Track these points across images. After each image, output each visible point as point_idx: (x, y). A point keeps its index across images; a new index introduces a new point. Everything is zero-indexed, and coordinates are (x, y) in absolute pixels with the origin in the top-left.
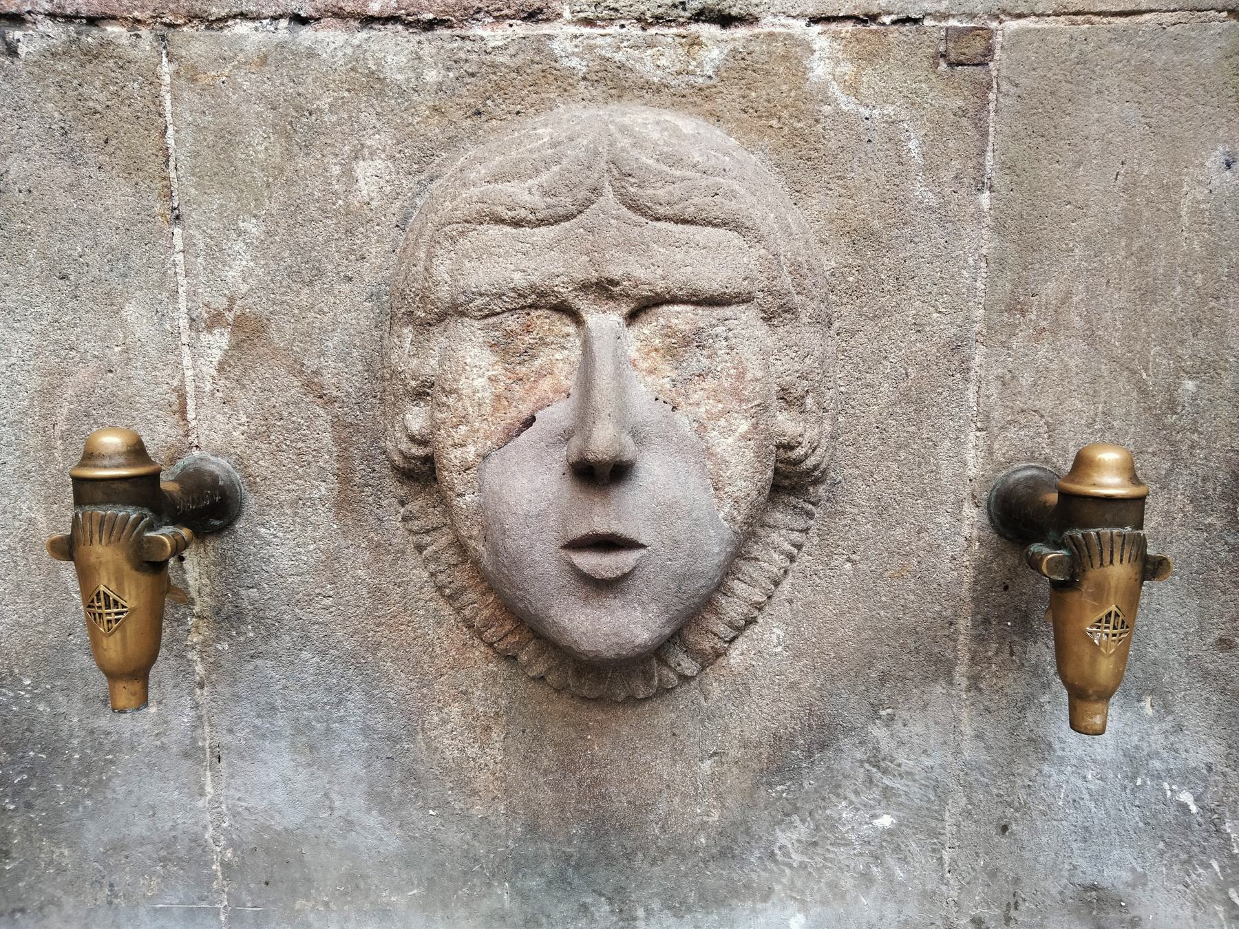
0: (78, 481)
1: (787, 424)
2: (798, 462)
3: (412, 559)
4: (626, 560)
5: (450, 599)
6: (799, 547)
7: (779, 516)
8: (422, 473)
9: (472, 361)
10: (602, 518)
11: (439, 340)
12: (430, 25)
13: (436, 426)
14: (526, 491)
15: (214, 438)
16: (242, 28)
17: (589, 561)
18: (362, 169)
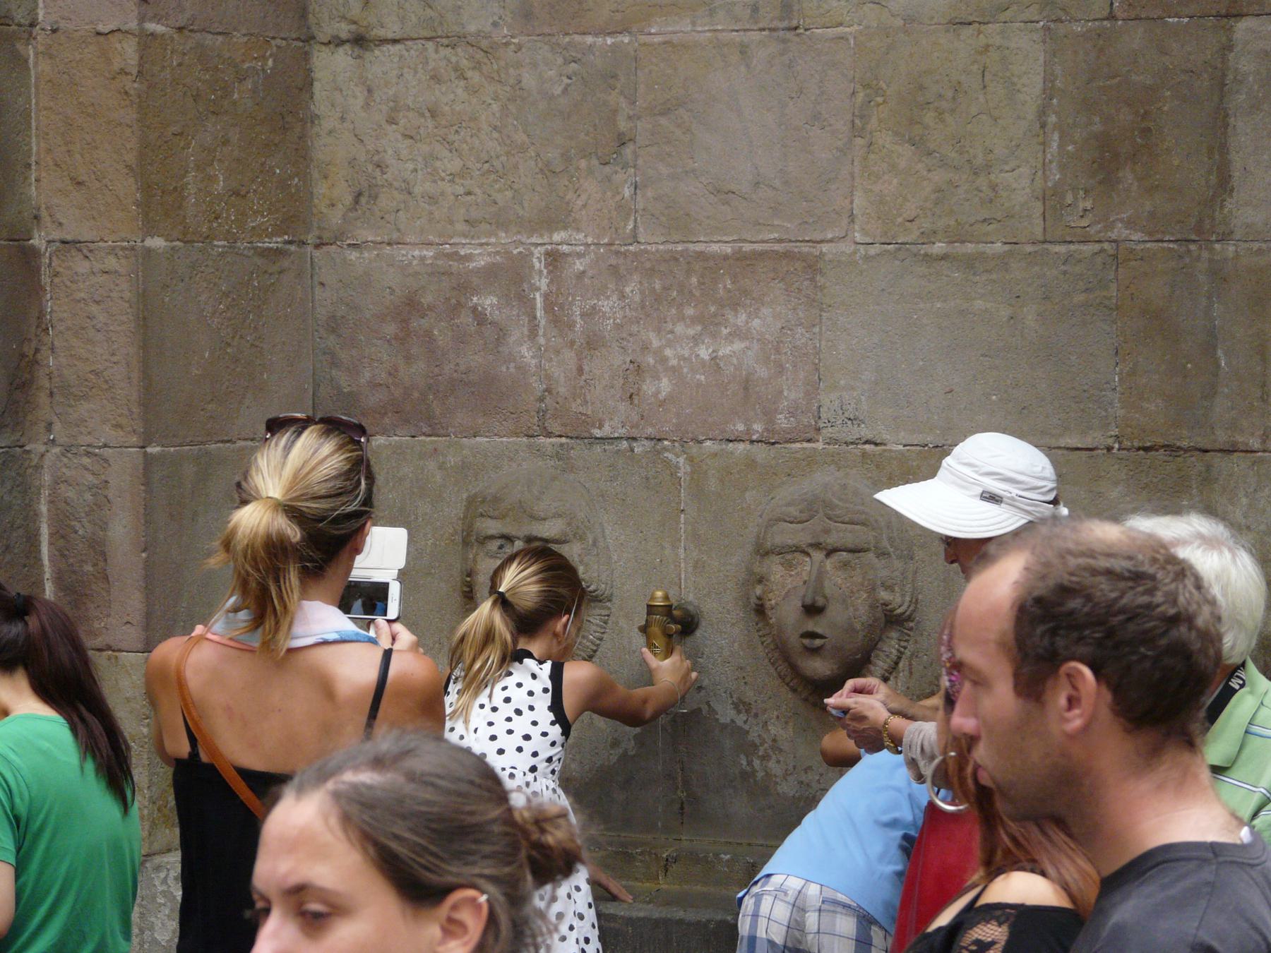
0: (649, 606)
1: (884, 595)
2: (891, 611)
3: (760, 648)
4: (818, 642)
5: (773, 664)
6: (905, 648)
7: (894, 634)
8: (760, 610)
9: (775, 569)
10: (811, 626)
11: (767, 561)
12: (773, 444)
13: (764, 592)
14: (788, 614)
15: (689, 595)
16: (708, 443)
17: (806, 642)
18: (747, 494)
